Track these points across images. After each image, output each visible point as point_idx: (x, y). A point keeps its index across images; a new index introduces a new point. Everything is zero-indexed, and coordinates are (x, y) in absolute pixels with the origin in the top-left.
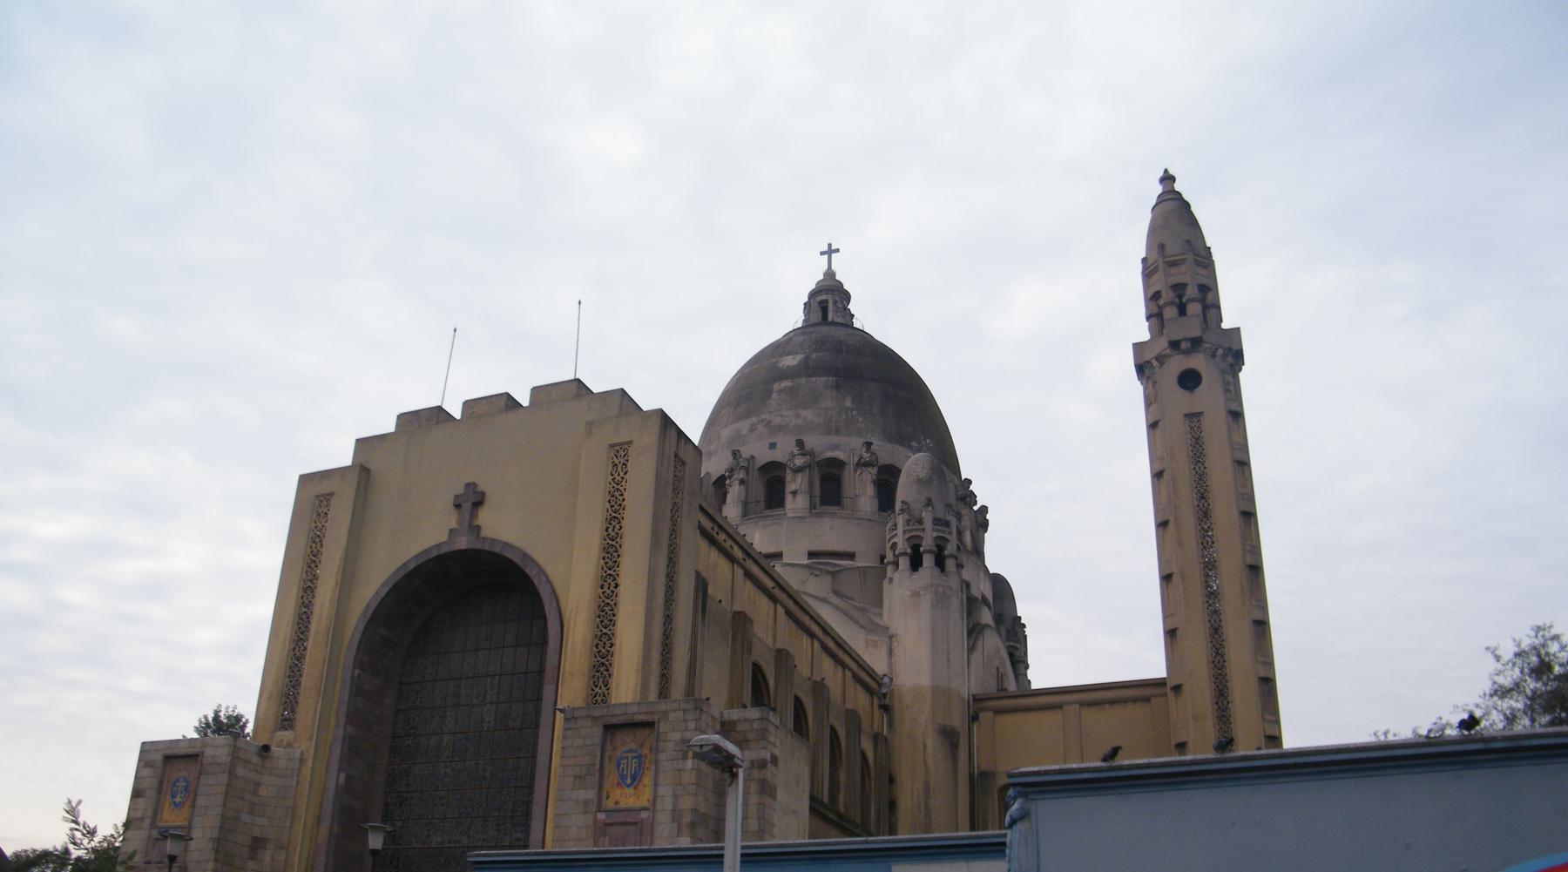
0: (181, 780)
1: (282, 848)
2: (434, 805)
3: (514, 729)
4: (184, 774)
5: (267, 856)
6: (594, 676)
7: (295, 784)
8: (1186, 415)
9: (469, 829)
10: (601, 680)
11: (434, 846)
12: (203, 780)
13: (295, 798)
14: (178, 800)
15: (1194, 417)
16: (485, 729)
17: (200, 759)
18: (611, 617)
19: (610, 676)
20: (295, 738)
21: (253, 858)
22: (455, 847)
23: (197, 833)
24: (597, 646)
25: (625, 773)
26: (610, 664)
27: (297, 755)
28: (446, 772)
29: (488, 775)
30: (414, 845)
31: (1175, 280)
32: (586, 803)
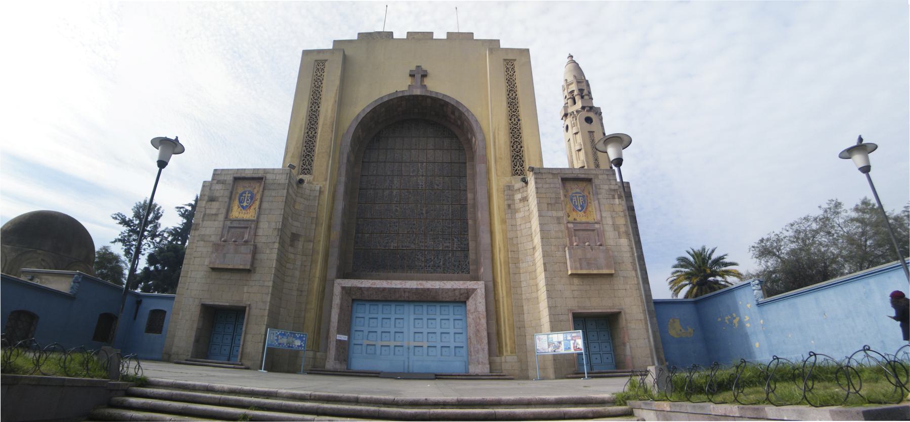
0: (247, 193)
1: (310, 241)
2: (390, 226)
3: (438, 189)
4: (249, 189)
5: (300, 245)
6: (513, 161)
7: (317, 205)
8: (589, 132)
9: (414, 240)
10: (518, 163)
11: (392, 248)
12: (266, 192)
13: (317, 212)
14: (245, 204)
15: (591, 133)
16: (420, 188)
17: (264, 180)
18: (519, 134)
19: (523, 161)
20: (314, 179)
21: (292, 246)
22: (407, 249)
23: (264, 225)
24: (513, 147)
25: (576, 204)
26: (522, 156)
27: (318, 188)
28: (397, 209)
29: (424, 212)
30: (379, 248)
31: (580, 88)
32: (558, 218)
